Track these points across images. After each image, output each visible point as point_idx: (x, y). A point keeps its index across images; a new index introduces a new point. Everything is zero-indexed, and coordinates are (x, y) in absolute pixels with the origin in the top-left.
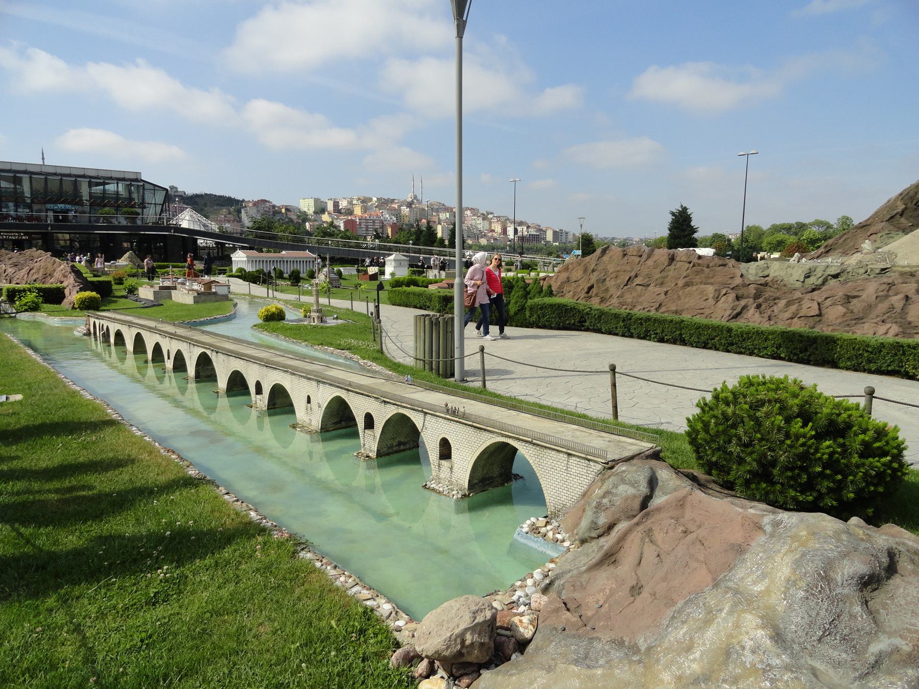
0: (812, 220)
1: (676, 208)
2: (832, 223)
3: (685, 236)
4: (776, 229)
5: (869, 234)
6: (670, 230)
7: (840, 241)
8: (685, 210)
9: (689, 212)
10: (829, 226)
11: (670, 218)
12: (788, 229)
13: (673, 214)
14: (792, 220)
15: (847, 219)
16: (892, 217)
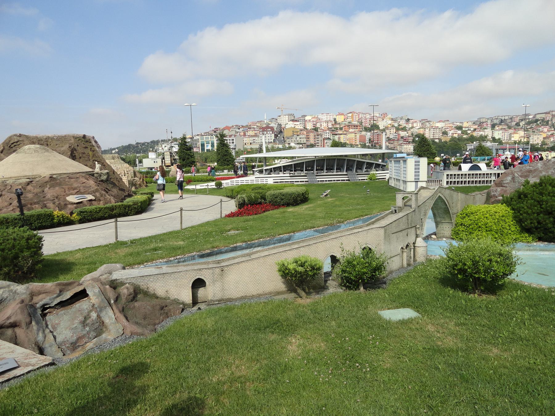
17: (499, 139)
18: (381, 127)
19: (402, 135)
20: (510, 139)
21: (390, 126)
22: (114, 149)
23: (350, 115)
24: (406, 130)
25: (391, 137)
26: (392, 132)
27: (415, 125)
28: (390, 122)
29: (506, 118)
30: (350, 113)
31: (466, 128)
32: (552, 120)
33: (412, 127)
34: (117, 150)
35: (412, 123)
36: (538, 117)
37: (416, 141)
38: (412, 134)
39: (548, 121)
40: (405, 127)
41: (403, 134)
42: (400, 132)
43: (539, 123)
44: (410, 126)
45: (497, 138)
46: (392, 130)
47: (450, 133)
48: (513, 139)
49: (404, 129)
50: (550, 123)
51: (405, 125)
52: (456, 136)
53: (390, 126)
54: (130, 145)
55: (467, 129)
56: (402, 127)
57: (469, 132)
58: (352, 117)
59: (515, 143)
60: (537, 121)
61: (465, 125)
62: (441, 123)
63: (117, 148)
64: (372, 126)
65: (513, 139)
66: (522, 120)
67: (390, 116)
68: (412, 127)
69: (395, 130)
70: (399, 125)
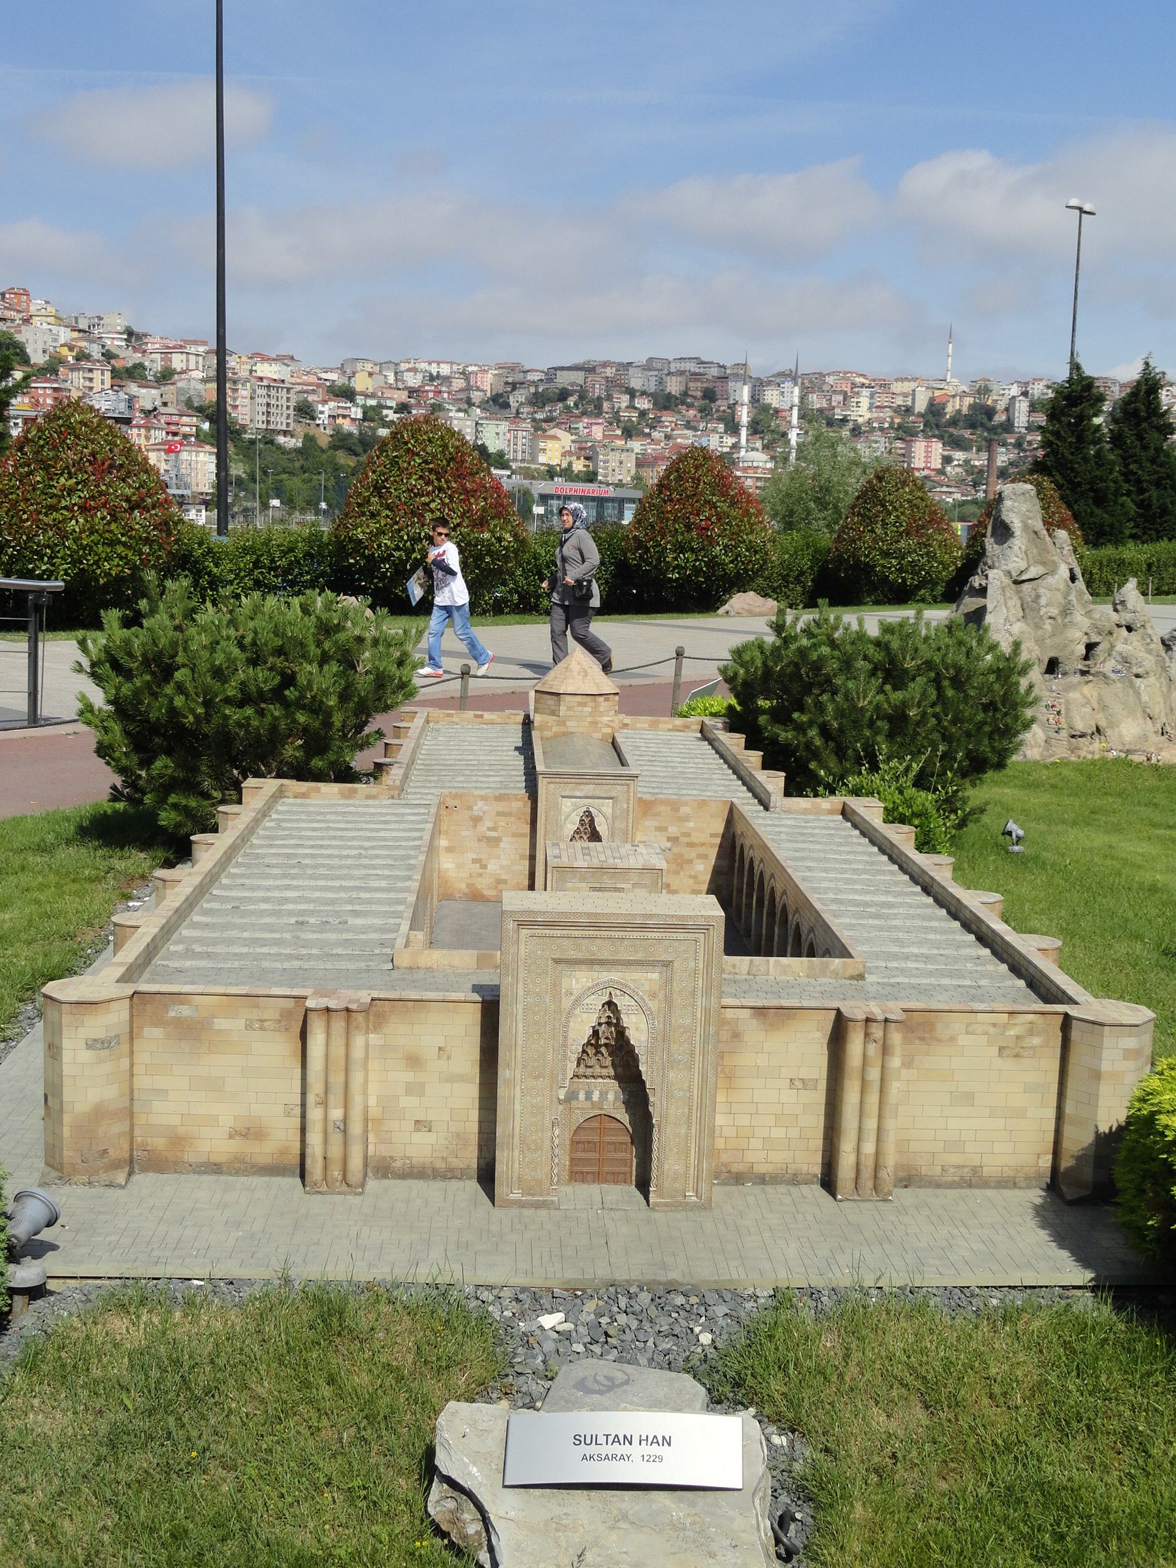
17: (501, 454)
18: (38, 358)
20: (534, 460)
21: (65, 351)
26: (97, 385)
27: (177, 362)
28: (65, 335)
29: (445, 370)
31: (367, 396)
32: (609, 398)
35: (167, 353)
36: (564, 380)
37: (206, 435)
39: (599, 398)
41: (147, 397)
42: (133, 388)
43: (571, 402)
45: (492, 450)
46: (96, 375)
47: (325, 410)
48: (542, 459)
49: (135, 373)
50: (606, 405)
52: (347, 426)
53: (65, 351)
55: (372, 402)
57: (391, 416)
59: (551, 473)
60: (563, 395)
61: (361, 383)
65: (542, 459)
66: (514, 386)
67: (36, 305)
69: (108, 375)
70: (108, 356)
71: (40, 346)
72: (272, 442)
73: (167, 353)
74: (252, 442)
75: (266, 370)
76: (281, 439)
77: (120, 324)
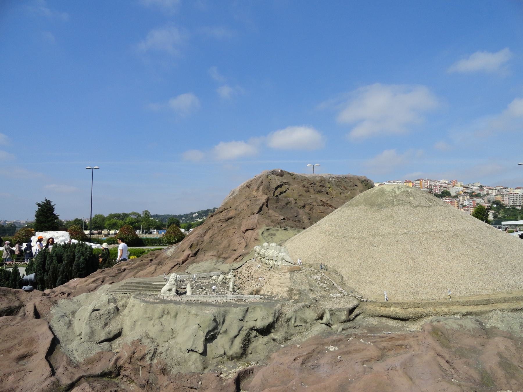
0: (130, 212)
1: (42, 200)
2: (140, 213)
3: (49, 221)
4: (112, 216)
5: (243, 229)
6: (36, 216)
7: (206, 238)
8: (48, 203)
9: (52, 204)
10: (139, 215)
11: (37, 208)
12: (118, 216)
13: (39, 205)
14: (120, 212)
15: (147, 211)
16: (261, 209)
18: (453, 194)
19: (478, 202)
21: (461, 192)
22: (195, 213)
23: (418, 182)
24: (480, 197)
25: (466, 203)
26: (466, 199)
28: (461, 189)
30: (418, 180)
33: (488, 194)
34: (197, 214)
35: (487, 190)
38: (489, 201)
40: (480, 194)
42: (475, 199)
44: (485, 192)
46: (465, 197)
49: (478, 196)
51: (479, 192)
53: (461, 192)
54: (208, 210)
56: (476, 194)
58: (420, 184)
62: (519, 190)
63: (197, 213)
64: (443, 193)
67: (460, 183)
68: (488, 194)
69: (468, 197)
71: (454, 192)
72: (514, 208)
73: (487, 190)
74: (508, 209)
75: (517, 191)
76: (517, 207)
77: (479, 185)
